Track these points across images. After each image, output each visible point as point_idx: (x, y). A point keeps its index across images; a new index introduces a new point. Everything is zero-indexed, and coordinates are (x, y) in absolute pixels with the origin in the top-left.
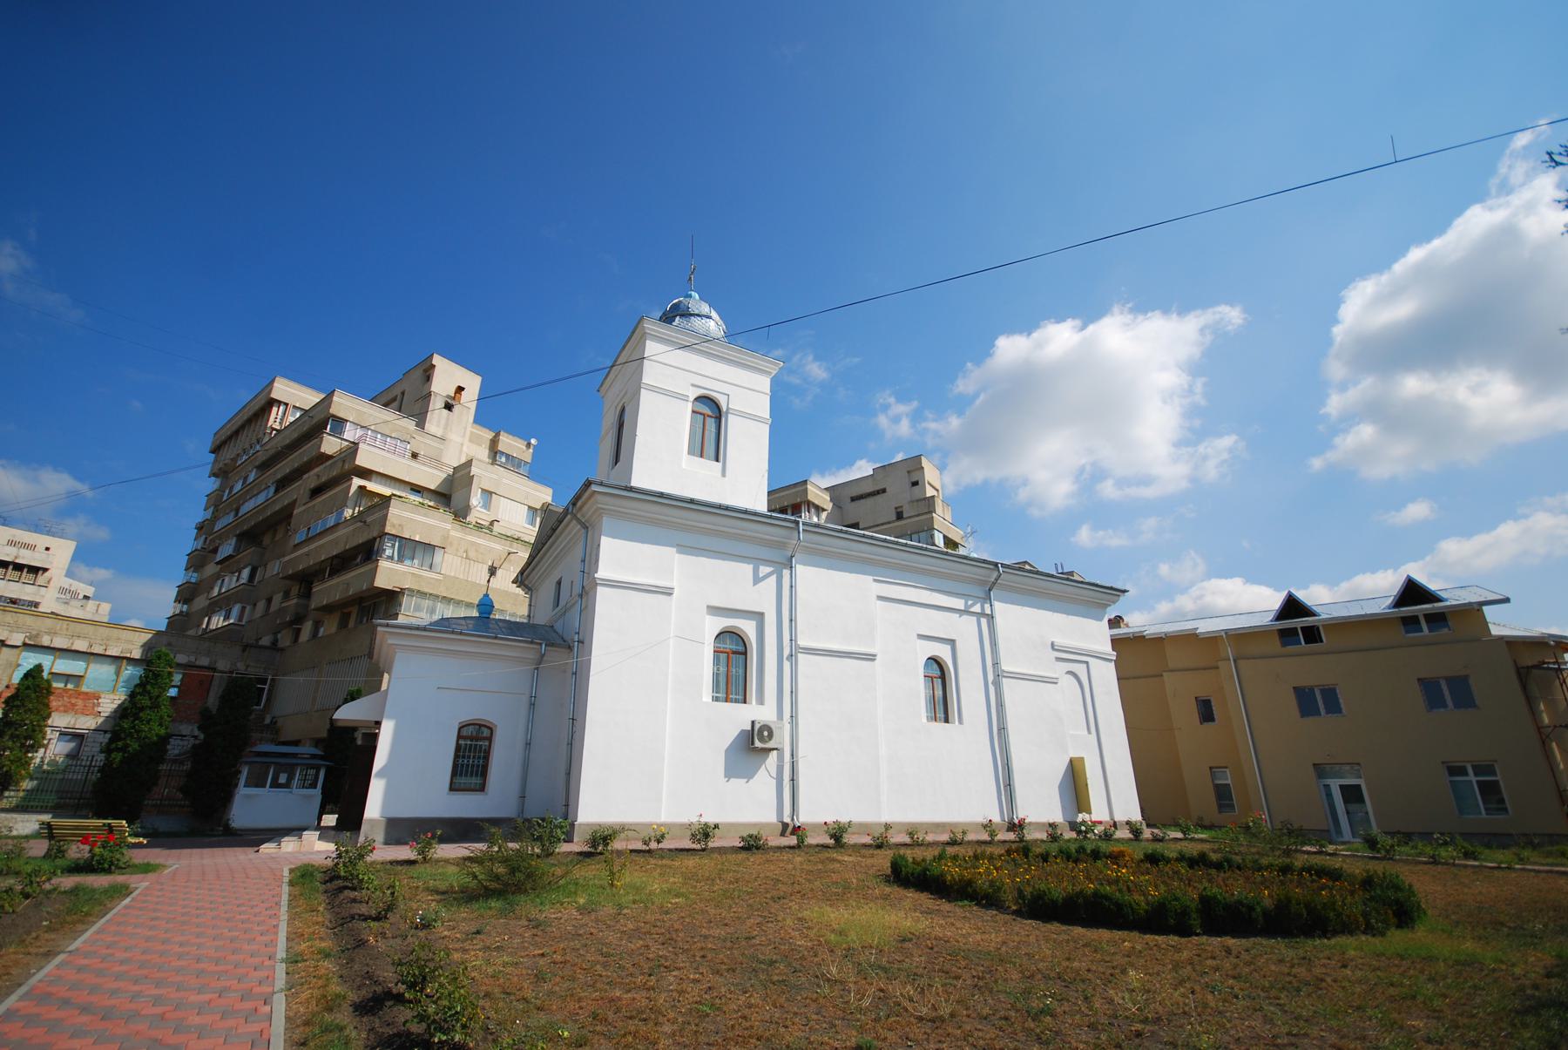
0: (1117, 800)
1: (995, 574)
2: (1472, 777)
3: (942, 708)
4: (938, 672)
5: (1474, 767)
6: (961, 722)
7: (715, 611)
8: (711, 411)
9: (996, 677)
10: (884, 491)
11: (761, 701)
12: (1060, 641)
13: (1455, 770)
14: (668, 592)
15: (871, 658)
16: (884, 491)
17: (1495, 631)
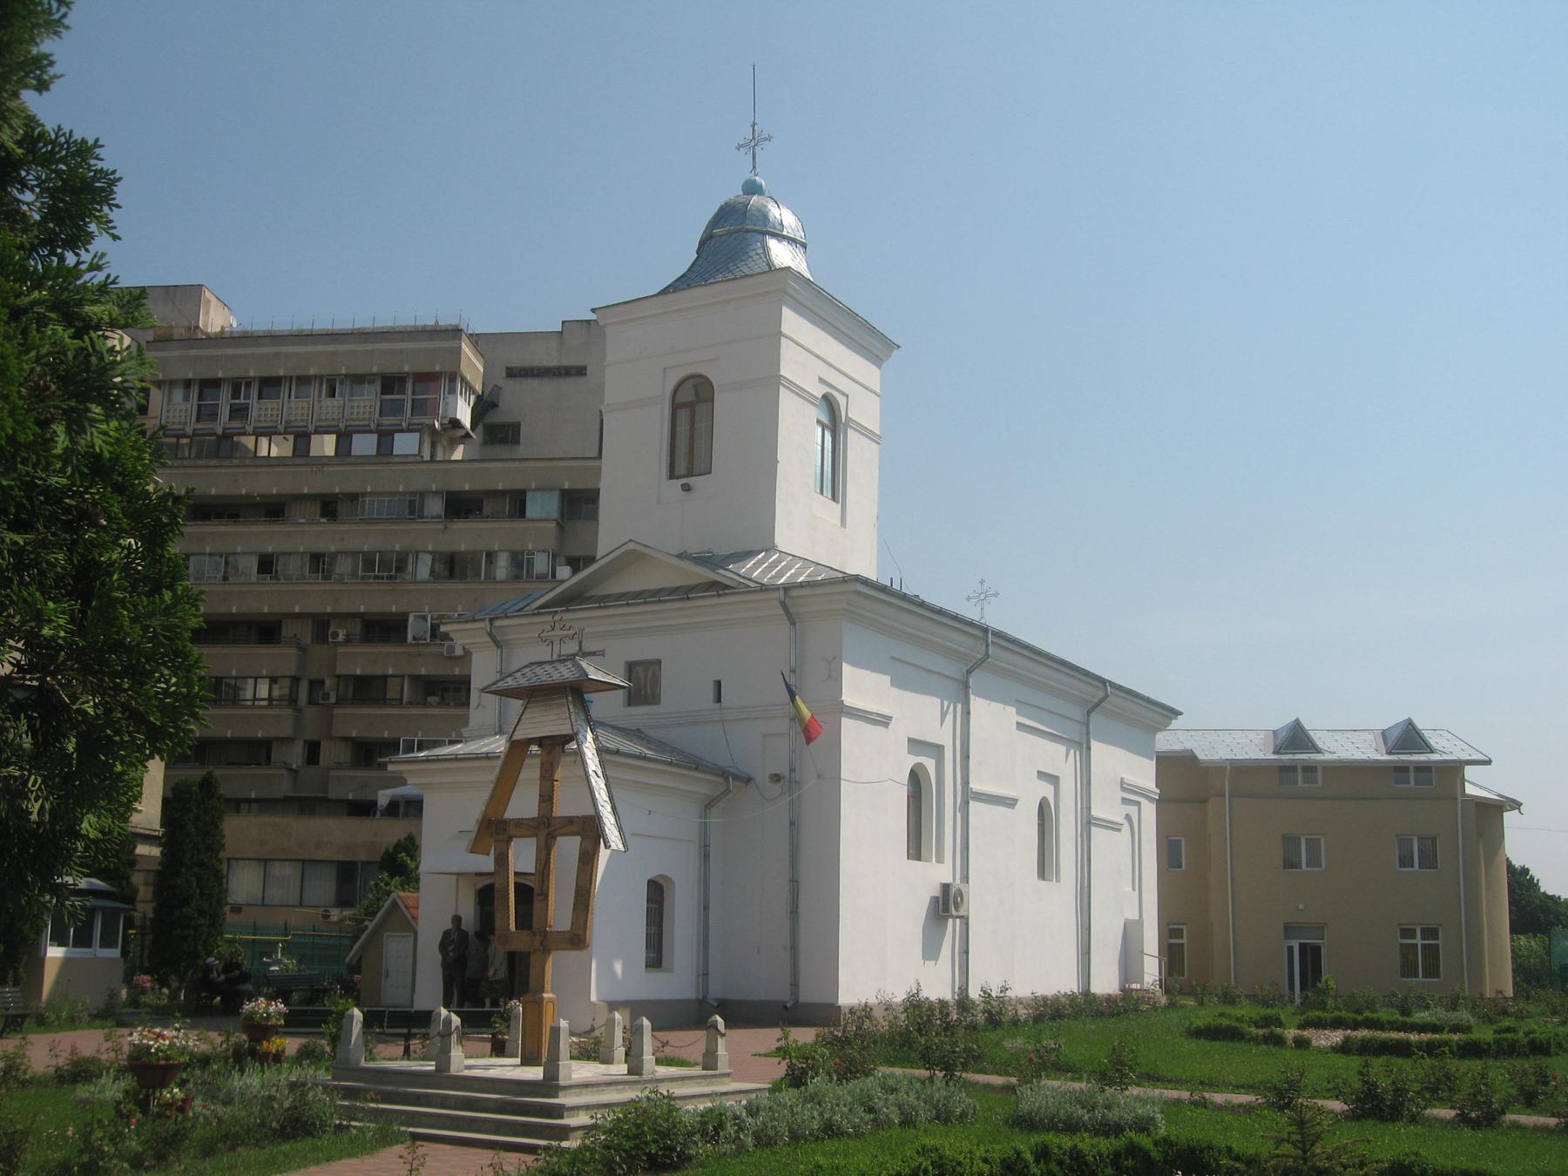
0: (1151, 971)
1: (1101, 694)
2: (1419, 941)
3: (1045, 867)
4: (1045, 815)
5: (1423, 930)
6: (1058, 880)
7: (916, 745)
8: (834, 420)
9: (1088, 822)
11: (940, 860)
12: (1131, 779)
13: (1407, 933)
14: (883, 721)
15: (1010, 802)
16: (581, 371)
17: (1470, 790)
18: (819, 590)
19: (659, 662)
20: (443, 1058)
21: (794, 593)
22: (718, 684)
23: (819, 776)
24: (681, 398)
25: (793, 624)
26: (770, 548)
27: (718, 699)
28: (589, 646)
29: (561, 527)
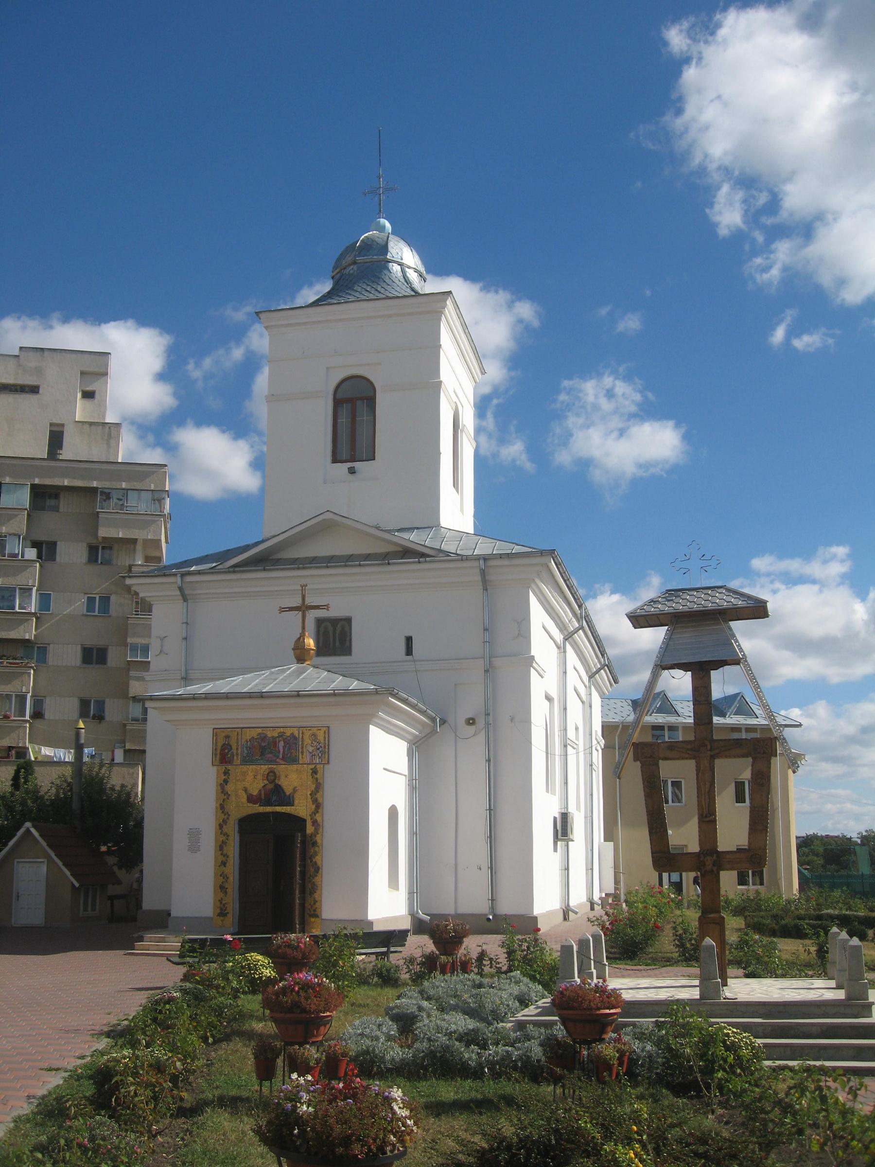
10: (34, 390)
16: (34, 390)
18: (516, 562)
19: (348, 620)
20: (710, 988)
21: (491, 563)
22: (409, 640)
23: (512, 720)
24: (338, 396)
25: (485, 589)
26: (438, 525)
27: (409, 651)
28: (309, 601)
29: (29, 515)
